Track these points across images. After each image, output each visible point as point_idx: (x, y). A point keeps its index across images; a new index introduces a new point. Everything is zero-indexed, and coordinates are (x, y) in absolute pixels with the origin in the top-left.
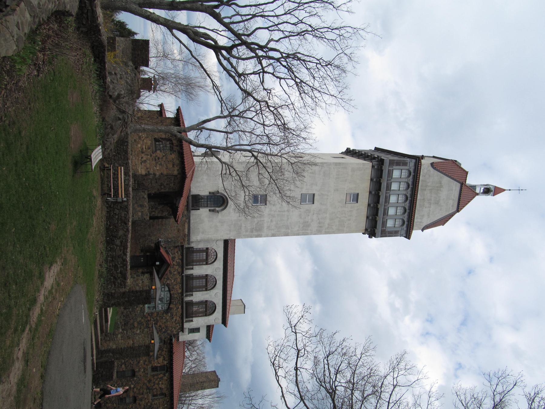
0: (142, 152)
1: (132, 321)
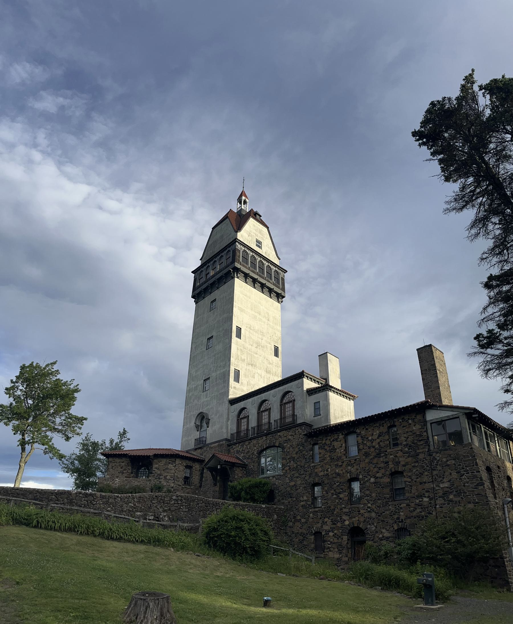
1: (289, 489)
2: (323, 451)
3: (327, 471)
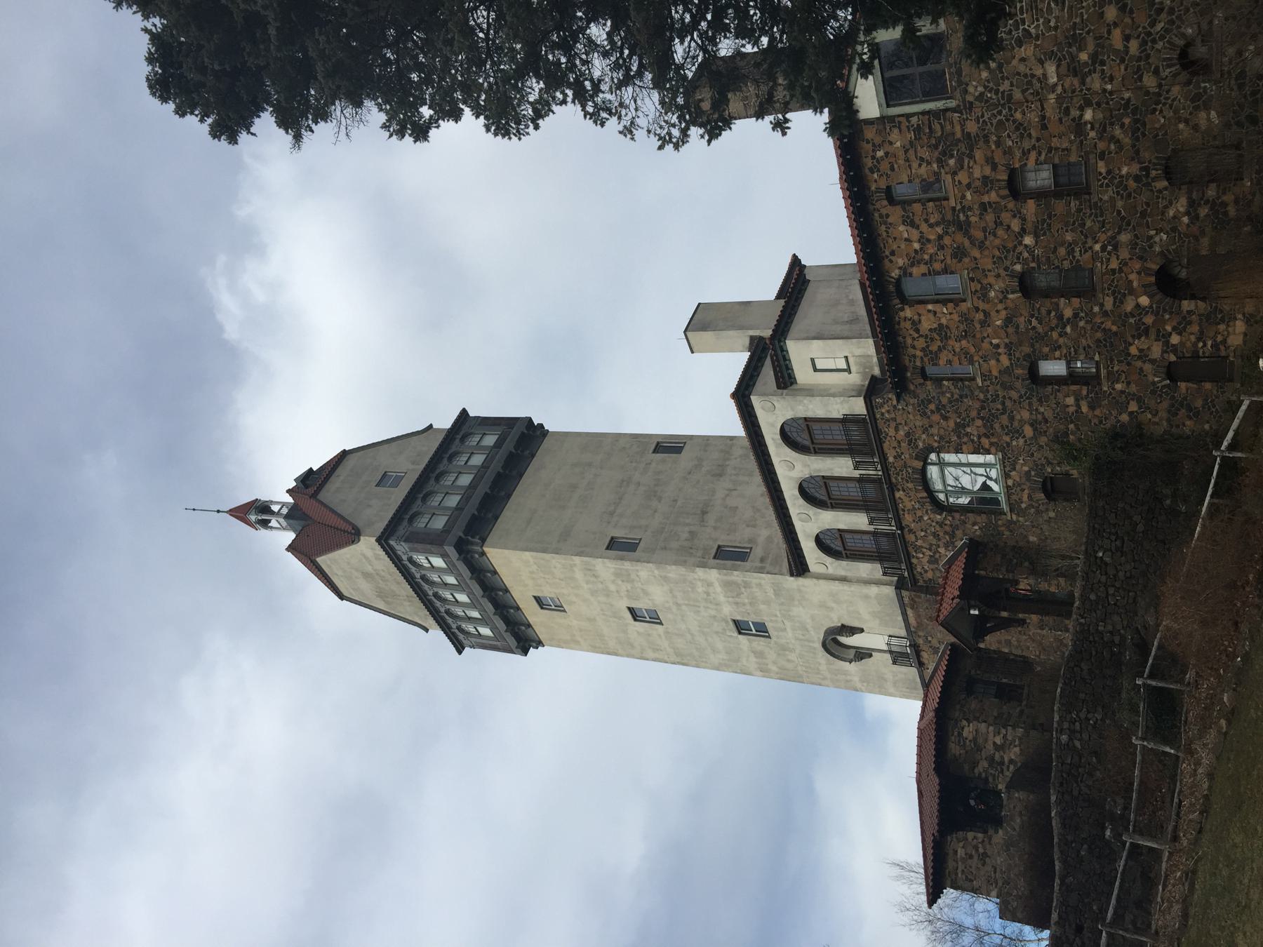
2: (944, 357)
3: (997, 346)
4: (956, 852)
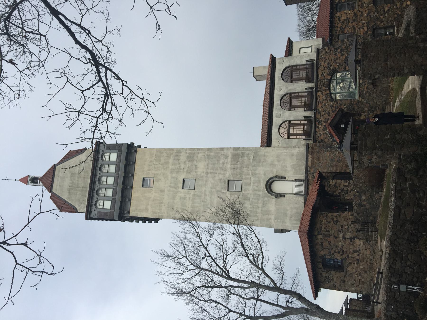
0: (358, 260)
3: (364, 23)
4: (322, 221)
